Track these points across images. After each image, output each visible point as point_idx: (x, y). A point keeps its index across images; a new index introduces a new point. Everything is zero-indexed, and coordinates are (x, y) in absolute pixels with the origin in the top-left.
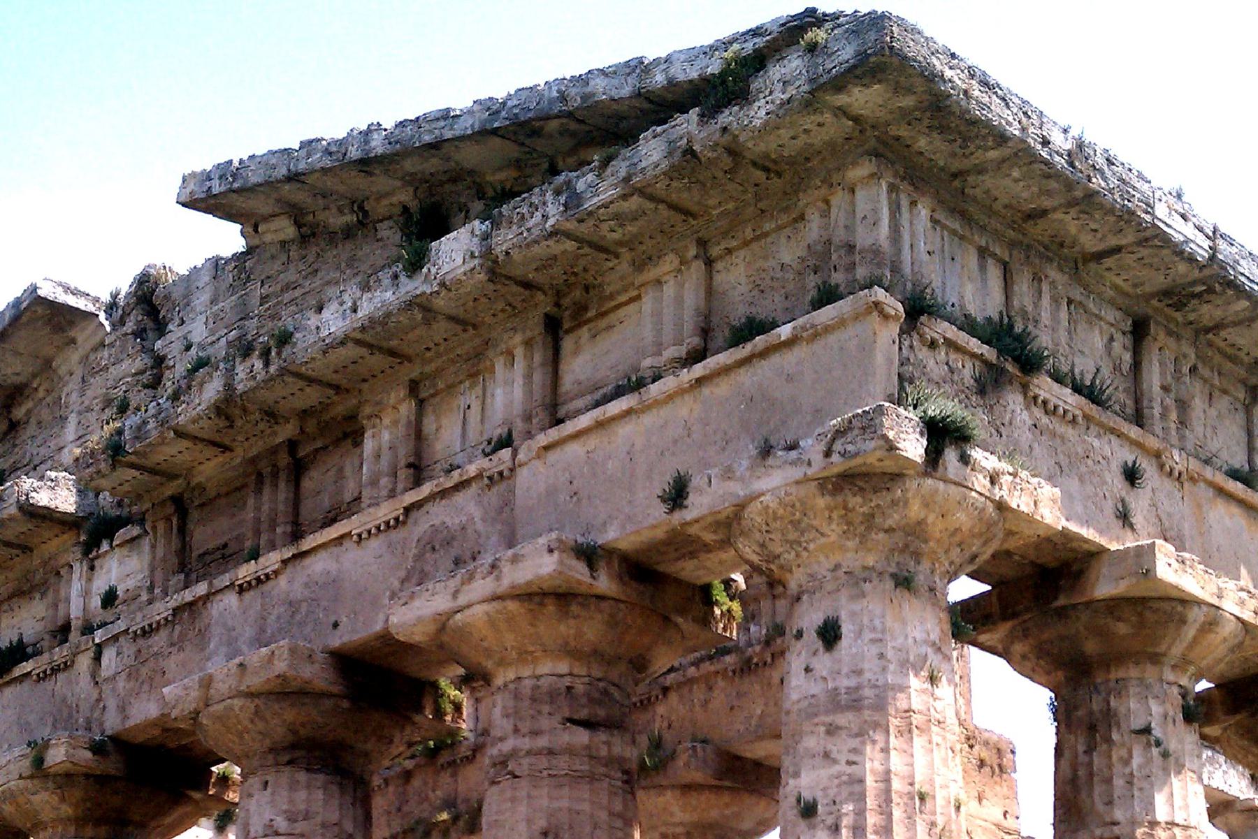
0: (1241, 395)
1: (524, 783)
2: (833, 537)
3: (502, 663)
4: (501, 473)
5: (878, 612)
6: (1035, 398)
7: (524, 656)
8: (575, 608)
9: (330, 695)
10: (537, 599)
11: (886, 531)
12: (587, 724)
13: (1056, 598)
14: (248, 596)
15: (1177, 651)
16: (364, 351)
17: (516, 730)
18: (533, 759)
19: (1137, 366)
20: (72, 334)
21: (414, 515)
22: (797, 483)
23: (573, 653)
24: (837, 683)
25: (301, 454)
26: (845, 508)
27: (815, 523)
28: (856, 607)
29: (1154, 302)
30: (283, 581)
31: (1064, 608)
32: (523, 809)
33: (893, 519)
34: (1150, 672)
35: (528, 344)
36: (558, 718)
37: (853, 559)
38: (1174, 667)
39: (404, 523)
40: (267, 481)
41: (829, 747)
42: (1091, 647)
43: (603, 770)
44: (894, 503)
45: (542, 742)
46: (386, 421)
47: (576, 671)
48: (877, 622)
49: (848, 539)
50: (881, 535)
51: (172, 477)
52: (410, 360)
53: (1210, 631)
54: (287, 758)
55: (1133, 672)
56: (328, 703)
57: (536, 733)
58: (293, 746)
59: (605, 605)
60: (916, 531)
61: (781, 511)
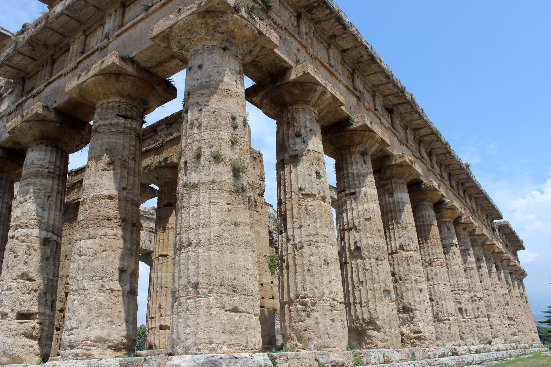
0: (326, 45)
1: (101, 134)
2: (202, 35)
3: (99, 99)
4: (104, 46)
5: (218, 58)
6: (270, 17)
7: (106, 96)
8: (121, 78)
9: (54, 122)
10: (108, 75)
11: (221, 33)
12: (125, 117)
13: (276, 83)
14: (35, 98)
15: (313, 101)
16: (68, 19)
17: (100, 119)
18: (105, 127)
19: (298, 25)
20: (5, 42)
21: (80, 65)
22: (190, 15)
23: (122, 95)
24: (202, 80)
25: (54, 58)
26: (206, 23)
27: (196, 30)
28: (210, 57)
29: (303, 10)
30: (44, 92)
31: (279, 85)
32: (99, 142)
33: (223, 28)
34: (306, 107)
35: (116, 11)
36: (114, 114)
37: (209, 43)
38: (313, 106)
39: (77, 67)
40: (45, 67)
41: (199, 101)
43: (128, 131)
44: (223, 22)
45: (108, 122)
46: (76, 42)
47: (122, 101)
48: (217, 62)
49: (208, 36)
50: (219, 35)
51: (21, 71)
52: (84, 24)
53: (323, 95)
54: (40, 142)
55: (301, 106)
56: (52, 124)
57: (107, 119)
58: (42, 138)
59: (131, 78)
60: (231, 34)
61: (184, 26)
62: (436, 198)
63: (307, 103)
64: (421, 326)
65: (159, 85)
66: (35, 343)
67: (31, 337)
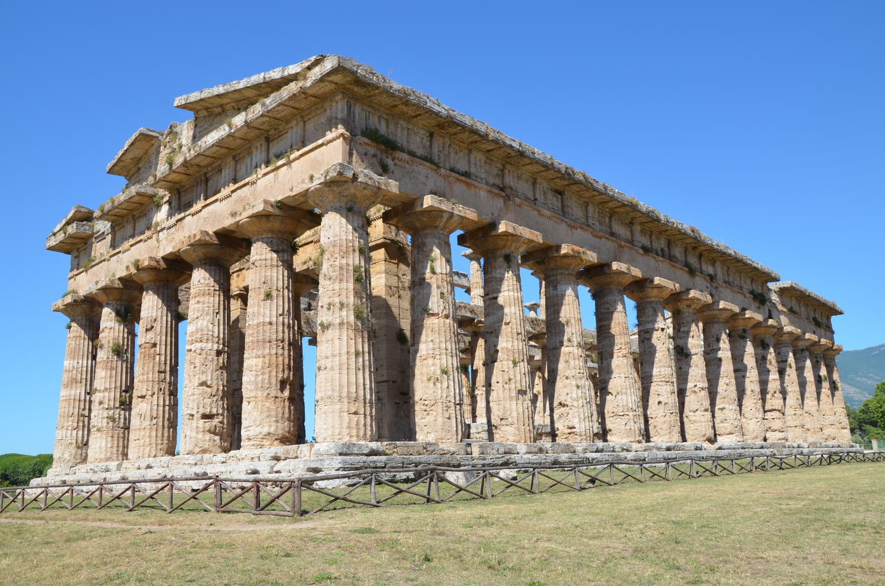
8: (271, 219)
15: (442, 224)
23: (272, 231)
42: (418, 225)
45: (263, 257)
58: (205, 259)
62: (624, 281)
63: (436, 227)
64: (575, 422)
65: (304, 218)
66: (217, 438)
67: (215, 433)
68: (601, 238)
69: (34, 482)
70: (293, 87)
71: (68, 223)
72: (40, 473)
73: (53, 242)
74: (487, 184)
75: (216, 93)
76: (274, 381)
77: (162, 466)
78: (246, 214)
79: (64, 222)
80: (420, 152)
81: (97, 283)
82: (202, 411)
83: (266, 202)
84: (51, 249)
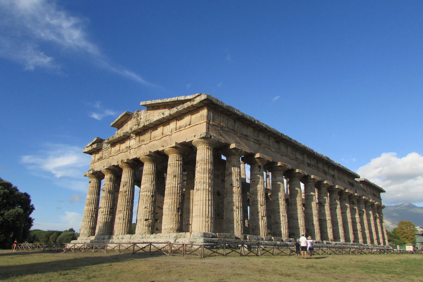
68: (292, 160)
69: (73, 242)
70: (189, 104)
71: (93, 144)
72: (76, 239)
73: (86, 150)
74: (253, 139)
75: (158, 102)
76: (175, 208)
77: (127, 238)
78: (168, 147)
79: (91, 143)
80: (231, 128)
81: (104, 167)
82: (145, 218)
83: (176, 143)
84: (85, 152)
